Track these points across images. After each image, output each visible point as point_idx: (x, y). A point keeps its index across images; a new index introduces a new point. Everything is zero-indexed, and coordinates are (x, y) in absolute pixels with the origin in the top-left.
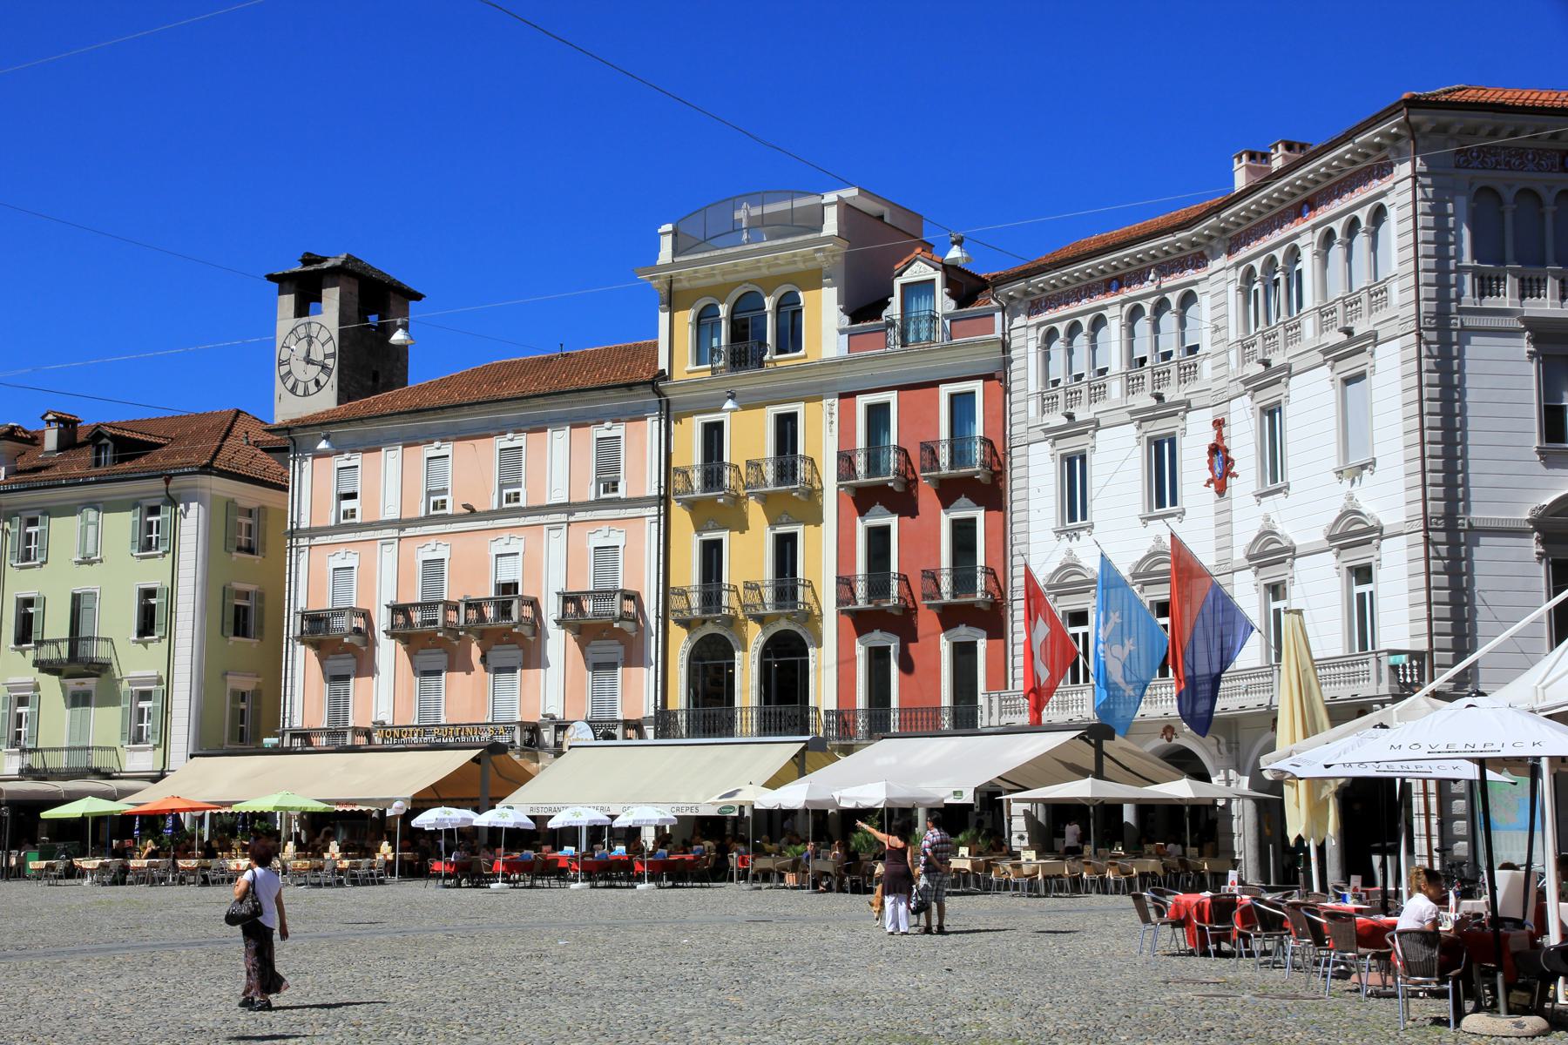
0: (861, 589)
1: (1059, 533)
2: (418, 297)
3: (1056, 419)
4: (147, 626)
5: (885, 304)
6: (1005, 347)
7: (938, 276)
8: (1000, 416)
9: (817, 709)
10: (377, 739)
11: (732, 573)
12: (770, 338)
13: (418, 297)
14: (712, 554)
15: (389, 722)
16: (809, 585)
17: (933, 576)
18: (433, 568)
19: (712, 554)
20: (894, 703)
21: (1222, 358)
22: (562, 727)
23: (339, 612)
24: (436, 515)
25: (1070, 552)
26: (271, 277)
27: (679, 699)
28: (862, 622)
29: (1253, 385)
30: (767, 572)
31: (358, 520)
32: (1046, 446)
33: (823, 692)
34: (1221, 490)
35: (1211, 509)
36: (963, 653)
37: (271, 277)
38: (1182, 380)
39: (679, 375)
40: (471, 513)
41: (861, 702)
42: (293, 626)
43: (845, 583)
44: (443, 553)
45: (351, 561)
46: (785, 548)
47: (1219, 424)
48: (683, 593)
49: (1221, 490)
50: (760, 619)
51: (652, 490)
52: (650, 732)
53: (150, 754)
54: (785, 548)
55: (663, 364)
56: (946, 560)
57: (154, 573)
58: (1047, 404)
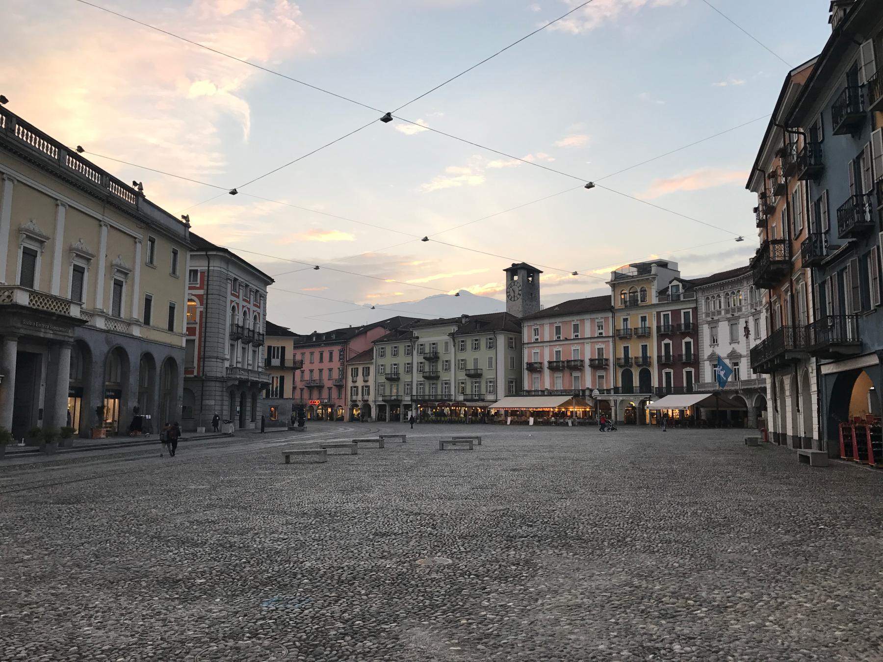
0: (663, 358)
1: (711, 346)
2: (542, 272)
3: (709, 319)
4: (490, 365)
5: (668, 291)
6: (696, 301)
7: (681, 285)
8: (696, 316)
9: (653, 387)
10: (546, 394)
11: (631, 355)
12: (639, 299)
13: (542, 272)
14: (626, 349)
15: (549, 389)
16: (650, 357)
17: (681, 355)
18: (558, 352)
19: (626, 349)
20: (672, 386)
21: (746, 307)
22: (591, 390)
23: (536, 363)
24: (559, 339)
25: (713, 351)
26: (504, 270)
27: (620, 384)
29: (753, 315)
30: (640, 355)
31: (539, 341)
32: (707, 325)
33: (655, 383)
34: (747, 337)
35: (745, 342)
36: (689, 374)
37: (504, 270)
38: (738, 311)
39: (616, 307)
40: (566, 339)
41: (664, 385)
42: (525, 367)
43: (659, 357)
44: (560, 349)
45: (538, 351)
46: (644, 348)
47: (746, 322)
48: (619, 359)
49: (747, 337)
50: (639, 366)
51: (611, 334)
52: (612, 392)
53: (493, 396)
54: (644, 348)
55: (613, 304)
56: (684, 352)
57: (493, 352)
58: (707, 315)
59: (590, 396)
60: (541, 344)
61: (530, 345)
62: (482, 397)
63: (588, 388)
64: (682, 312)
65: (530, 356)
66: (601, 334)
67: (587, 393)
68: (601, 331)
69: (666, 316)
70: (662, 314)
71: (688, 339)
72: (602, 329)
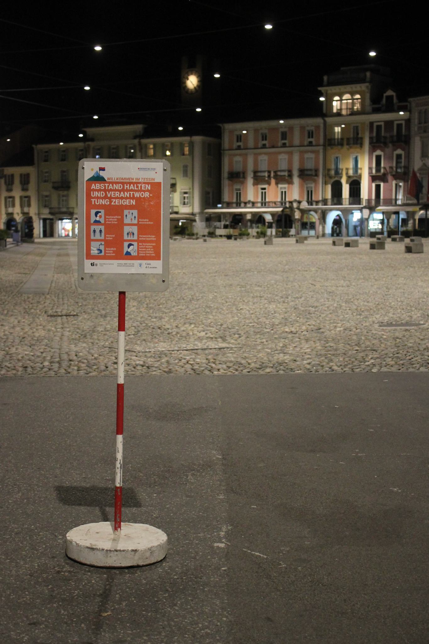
0: (374, 171)
9: (363, 199)
16: (361, 169)
20: (382, 197)
28: (373, 178)
33: (364, 194)
41: (373, 197)
43: (370, 169)
55: (324, 111)
59: (298, 208)
60: (244, 152)
61: (231, 152)
62: (175, 210)
63: (295, 201)
64: (396, 123)
65: (231, 164)
66: (311, 142)
67: (295, 205)
68: (310, 140)
69: (379, 127)
70: (375, 124)
71: (399, 151)
72: (312, 137)
